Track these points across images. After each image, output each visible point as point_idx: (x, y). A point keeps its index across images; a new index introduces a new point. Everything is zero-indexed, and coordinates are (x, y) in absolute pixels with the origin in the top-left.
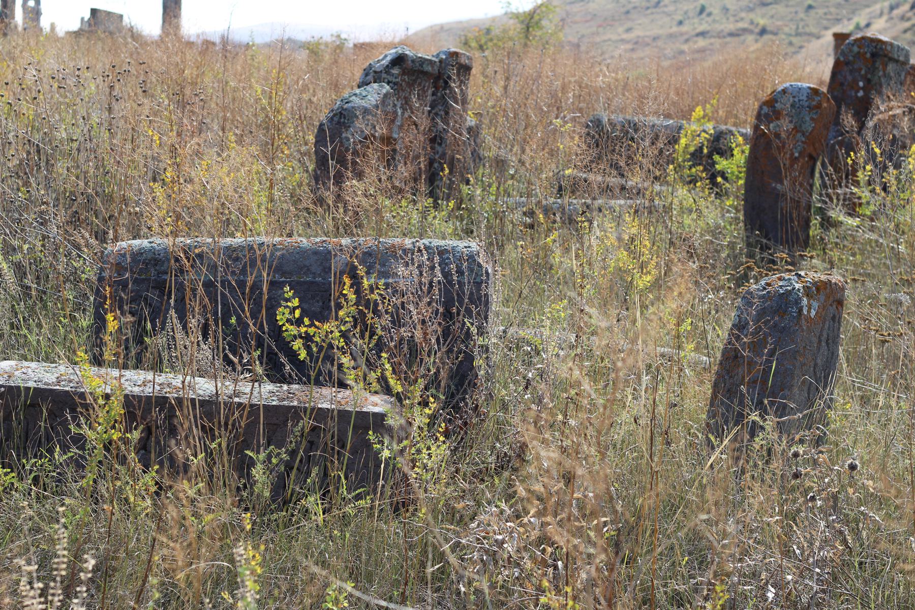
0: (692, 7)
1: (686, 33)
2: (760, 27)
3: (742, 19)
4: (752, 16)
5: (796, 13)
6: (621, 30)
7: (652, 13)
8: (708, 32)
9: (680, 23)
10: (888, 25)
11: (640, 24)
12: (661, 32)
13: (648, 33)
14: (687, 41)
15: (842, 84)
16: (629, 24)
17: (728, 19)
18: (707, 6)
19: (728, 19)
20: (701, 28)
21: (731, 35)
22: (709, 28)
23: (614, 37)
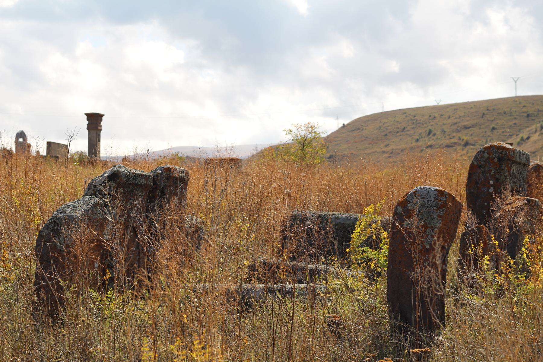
0: (424, 131)
1: (421, 146)
2: (464, 141)
3: (454, 137)
4: (459, 135)
5: (486, 132)
6: (382, 145)
7: (401, 135)
9: (417, 140)
10: (540, 137)
13: (398, 147)
15: (476, 183)
16: (387, 142)
17: (445, 137)
18: (433, 130)
19: (445, 137)
20: (430, 143)
21: (448, 146)
23: (379, 150)
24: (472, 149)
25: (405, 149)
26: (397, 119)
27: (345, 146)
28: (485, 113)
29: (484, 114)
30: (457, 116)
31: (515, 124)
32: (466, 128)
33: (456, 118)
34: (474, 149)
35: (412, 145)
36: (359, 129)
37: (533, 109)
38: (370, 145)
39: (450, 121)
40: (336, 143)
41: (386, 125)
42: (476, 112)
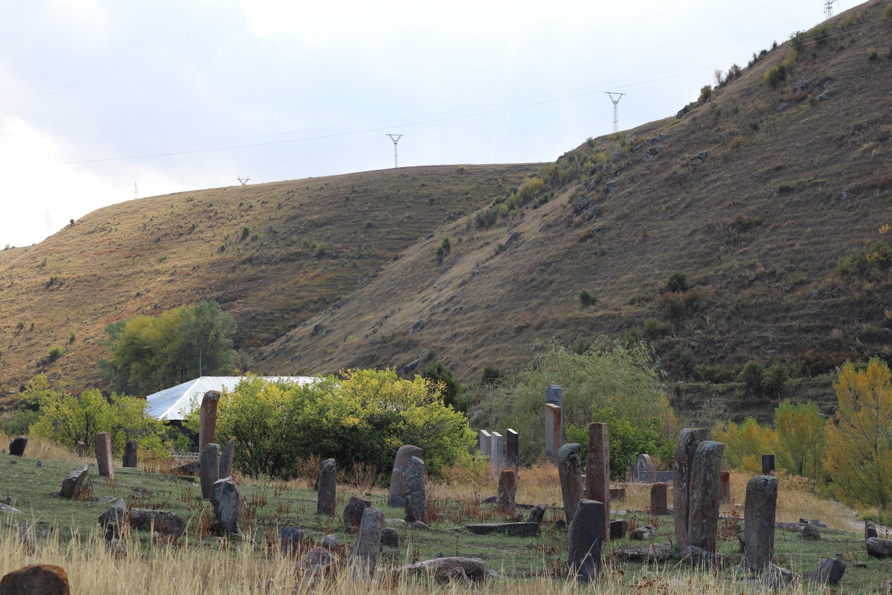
0: (233, 232)
1: (231, 260)
2: (316, 250)
3: (294, 243)
5: (355, 232)
7: (187, 241)
8: (257, 258)
11: (174, 253)
12: (200, 260)
14: (234, 269)
22: (257, 254)
23: (146, 269)
24: (332, 265)
25: (199, 267)
26: (176, 210)
27: (80, 262)
28: (351, 197)
29: (347, 198)
30: (295, 204)
31: (409, 217)
32: (316, 225)
33: (294, 207)
35: (214, 258)
36: (103, 229)
37: (440, 191)
38: (130, 260)
39: (281, 213)
40: (60, 255)
41: (156, 221)
42: (333, 196)
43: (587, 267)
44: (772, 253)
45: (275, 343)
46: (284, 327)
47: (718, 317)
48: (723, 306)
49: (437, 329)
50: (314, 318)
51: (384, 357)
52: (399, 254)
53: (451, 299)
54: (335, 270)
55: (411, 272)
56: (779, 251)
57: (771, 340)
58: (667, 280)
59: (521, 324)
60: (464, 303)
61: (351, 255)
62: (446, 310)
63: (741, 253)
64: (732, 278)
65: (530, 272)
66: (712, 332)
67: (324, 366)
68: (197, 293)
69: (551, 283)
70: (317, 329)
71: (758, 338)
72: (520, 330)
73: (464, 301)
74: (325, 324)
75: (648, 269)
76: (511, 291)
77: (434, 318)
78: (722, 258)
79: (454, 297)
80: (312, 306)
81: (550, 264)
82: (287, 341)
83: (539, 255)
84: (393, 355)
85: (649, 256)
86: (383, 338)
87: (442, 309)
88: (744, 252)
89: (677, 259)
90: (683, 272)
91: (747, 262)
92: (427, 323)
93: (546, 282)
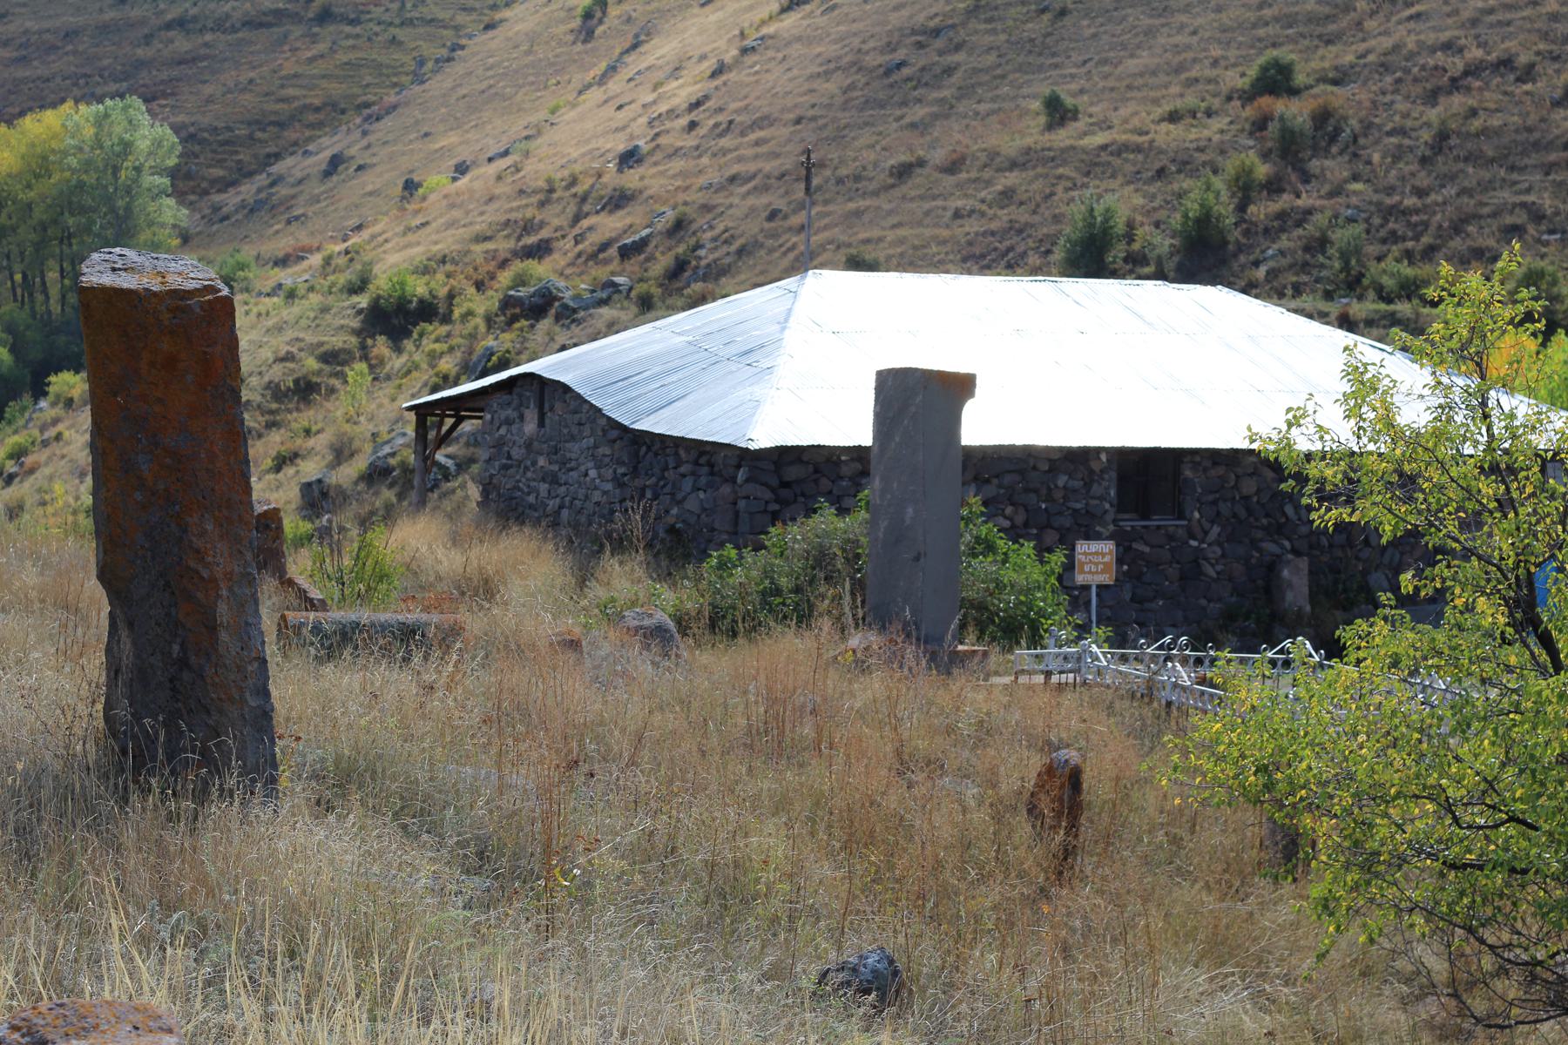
1: (143, 22)
8: (195, 19)
13: (46, 25)
14: (148, 39)
22: (194, 11)
24: (348, 37)
25: (76, 33)
34: (358, 36)
43: (1032, 40)
44: (1493, 18)
45: (243, 188)
46: (255, 156)
47: (1397, 155)
48: (1401, 131)
49: (678, 165)
50: (325, 141)
51: (556, 222)
52: (498, 16)
53: (698, 104)
54: (354, 47)
55: (529, 52)
56: (1508, 16)
57: (1549, 212)
58: (1253, 72)
59: (904, 157)
60: (736, 111)
61: (386, 17)
62: (693, 125)
63: (1411, 18)
64: (1407, 71)
65: (890, 47)
66: (1390, 190)
67: (411, 237)
68: (76, 84)
69: (949, 71)
70: (336, 162)
71: (1515, 205)
72: (903, 172)
73: (734, 106)
74: (353, 151)
75: (1188, 47)
76: (852, 87)
77: (662, 140)
78: (1370, 24)
79: (707, 97)
80: (312, 117)
81: (936, 32)
82: (272, 184)
83: (905, 13)
84: (577, 219)
85: (1183, 18)
86: (549, 181)
87: (683, 122)
88: (1418, 16)
89: (1254, 26)
90: (1286, 54)
91: (1431, 38)
92: (651, 153)
93: (938, 69)
